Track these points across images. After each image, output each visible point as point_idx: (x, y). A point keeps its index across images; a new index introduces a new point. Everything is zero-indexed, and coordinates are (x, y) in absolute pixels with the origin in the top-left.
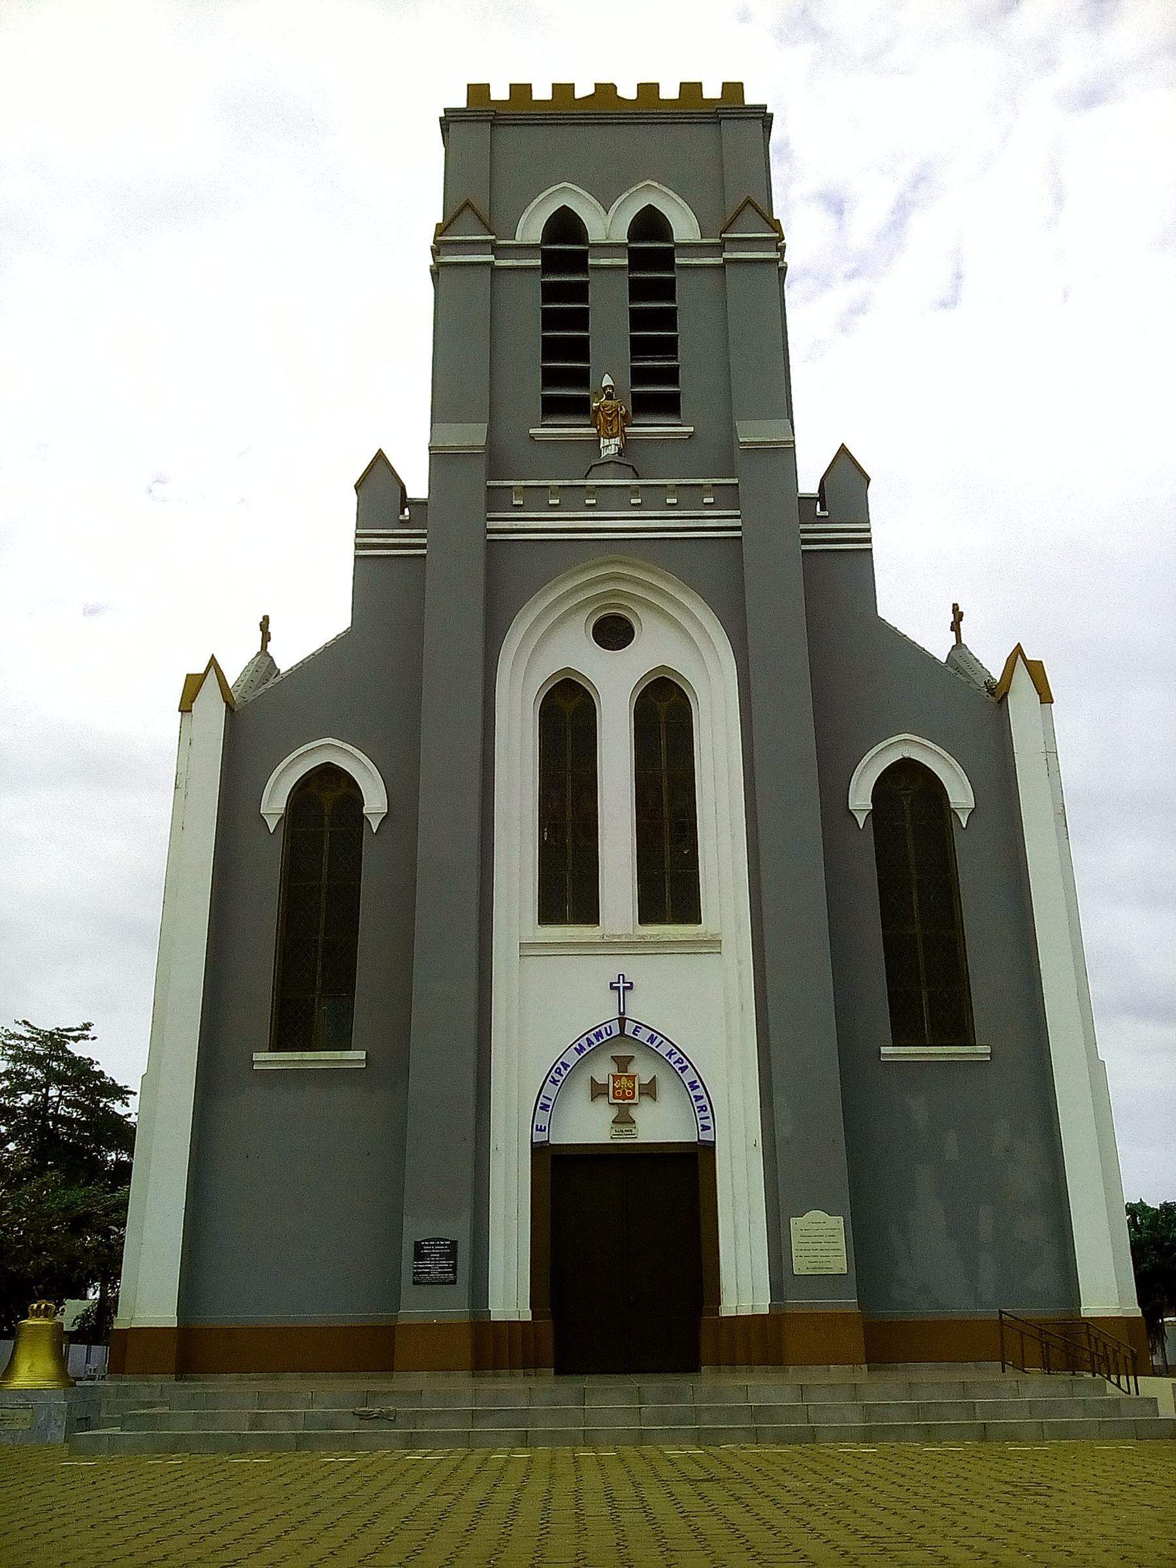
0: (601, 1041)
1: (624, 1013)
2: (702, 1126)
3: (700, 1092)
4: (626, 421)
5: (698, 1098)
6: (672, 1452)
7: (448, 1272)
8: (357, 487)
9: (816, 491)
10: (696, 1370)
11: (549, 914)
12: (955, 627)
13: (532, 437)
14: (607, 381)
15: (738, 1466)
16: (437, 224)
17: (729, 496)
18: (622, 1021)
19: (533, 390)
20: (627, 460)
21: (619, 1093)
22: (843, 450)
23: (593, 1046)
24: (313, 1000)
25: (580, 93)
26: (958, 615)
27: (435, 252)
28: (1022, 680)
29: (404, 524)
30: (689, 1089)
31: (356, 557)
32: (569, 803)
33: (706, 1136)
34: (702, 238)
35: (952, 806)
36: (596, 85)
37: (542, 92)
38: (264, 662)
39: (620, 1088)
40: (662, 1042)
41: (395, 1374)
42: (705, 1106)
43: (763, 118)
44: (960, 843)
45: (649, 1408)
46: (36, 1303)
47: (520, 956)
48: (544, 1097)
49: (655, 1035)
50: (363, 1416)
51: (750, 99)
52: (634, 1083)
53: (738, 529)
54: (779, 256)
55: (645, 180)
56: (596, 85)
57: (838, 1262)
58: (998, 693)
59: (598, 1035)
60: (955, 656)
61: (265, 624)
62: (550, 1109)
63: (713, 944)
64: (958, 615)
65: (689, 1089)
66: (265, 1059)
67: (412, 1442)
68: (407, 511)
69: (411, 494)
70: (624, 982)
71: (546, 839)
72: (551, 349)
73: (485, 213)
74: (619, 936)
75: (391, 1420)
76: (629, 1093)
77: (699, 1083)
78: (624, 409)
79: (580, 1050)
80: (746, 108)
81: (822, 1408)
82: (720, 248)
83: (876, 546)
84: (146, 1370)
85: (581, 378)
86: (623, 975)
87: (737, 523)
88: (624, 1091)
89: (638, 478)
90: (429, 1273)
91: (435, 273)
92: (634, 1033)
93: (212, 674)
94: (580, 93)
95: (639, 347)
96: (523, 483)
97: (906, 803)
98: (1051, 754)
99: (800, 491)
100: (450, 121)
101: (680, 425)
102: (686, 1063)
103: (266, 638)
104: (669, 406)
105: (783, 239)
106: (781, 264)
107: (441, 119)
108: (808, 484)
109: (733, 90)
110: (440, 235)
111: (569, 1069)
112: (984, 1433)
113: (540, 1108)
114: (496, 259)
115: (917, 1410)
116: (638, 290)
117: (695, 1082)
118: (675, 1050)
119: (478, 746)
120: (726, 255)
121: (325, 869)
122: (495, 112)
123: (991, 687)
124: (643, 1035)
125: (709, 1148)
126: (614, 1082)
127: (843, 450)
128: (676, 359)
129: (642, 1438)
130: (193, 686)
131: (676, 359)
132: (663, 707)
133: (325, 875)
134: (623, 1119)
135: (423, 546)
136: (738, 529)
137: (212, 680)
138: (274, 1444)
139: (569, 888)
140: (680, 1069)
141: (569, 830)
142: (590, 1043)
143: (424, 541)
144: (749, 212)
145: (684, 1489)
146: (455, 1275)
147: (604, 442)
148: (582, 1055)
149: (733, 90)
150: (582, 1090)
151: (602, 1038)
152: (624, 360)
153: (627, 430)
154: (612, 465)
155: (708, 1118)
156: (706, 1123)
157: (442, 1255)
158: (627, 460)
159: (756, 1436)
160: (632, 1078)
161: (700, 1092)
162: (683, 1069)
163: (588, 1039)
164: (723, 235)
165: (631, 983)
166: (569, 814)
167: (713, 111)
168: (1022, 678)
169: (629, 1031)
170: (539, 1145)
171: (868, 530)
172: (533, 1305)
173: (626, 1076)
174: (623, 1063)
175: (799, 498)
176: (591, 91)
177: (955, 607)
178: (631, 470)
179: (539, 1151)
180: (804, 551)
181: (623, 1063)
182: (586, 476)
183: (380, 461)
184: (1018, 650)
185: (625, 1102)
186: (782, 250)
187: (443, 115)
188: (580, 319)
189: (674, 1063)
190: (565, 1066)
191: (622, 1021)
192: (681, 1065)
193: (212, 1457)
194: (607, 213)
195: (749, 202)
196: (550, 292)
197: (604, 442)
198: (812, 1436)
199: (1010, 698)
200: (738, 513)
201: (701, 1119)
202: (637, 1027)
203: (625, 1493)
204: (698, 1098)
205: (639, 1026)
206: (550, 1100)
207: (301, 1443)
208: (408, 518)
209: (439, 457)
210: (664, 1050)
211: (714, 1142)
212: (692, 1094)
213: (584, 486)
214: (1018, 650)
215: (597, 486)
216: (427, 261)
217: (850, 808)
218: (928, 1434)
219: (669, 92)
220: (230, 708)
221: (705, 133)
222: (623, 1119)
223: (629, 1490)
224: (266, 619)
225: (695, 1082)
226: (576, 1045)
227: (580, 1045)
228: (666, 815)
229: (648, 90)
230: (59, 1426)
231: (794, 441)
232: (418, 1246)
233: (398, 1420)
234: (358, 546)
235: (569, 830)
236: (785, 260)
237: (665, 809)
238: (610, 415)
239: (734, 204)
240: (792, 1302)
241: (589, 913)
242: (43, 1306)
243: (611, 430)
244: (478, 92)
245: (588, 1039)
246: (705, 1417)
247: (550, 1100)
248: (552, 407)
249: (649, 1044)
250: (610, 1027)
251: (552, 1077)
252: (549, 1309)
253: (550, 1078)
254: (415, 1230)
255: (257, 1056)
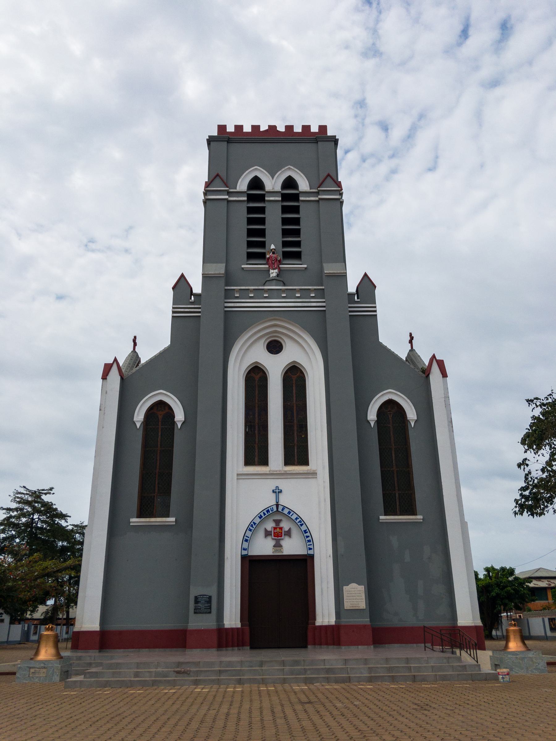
0: (269, 513)
1: (278, 502)
2: (309, 548)
3: (308, 534)
4: (280, 262)
5: (307, 537)
6: (296, 688)
7: (208, 609)
8: (173, 288)
9: (355, 291)
10: (305, 647)
11: (248, 462)
12: (411, 342)
13: (243, 268)
14: (273, 247)
15: (320, 695)
16: (206, 182)
17: (321, 294)
18: (277, 505)
19: (243, 249)
20: (279, 279)
21: (276, 535)
22: (366, 275)
23: (266, 516)
24: (154, 496)
25: (262, 129)
26: (412, 338)
27: (205, 194)
28: (435, 369)
29: (192, 303)
30: (304, 533)
31: (173, 317)
32: (256, 416)
33: (311, 552)
34: (310, 189)
35: (408, 419)
36: (269, 126)
37: (247, 129)
38: (134, 357)
39: (276, 532)
40: (293, 514)
41: (187, 650)
42: (310, 540)
43: (335, 141)
44: (412, 434)
45: (287, 668)
46: (47, 625)
47: (237, 479)
48: (246, 536)
49: (291, 511)
50: (178, 672)
51: (330, 133)
52: (282, 530)
53: (324, 307)
54: (340, 197)
55: (288, 165)
56: (269, 126)
57: (362, 604)
58: (426, 372)
59: (268, 511)
60: (411, 354)
61: (134, 341)
62: (248, 541)
63: (313, 474)
64: (412, 338)
65: (304, 533)
66: (135, 521)
67: (196, 683)
68: (193, 298)
69: (194, 291)
70: (278, 490)
71: (247, 431)
72: (250, 233)
73: (225, 178)
74: (276, 471)
75: (188, 674)
76: (280, 535)
77: (308, 531)
78: (279, 258)
79: (260, 517)
80: (328, 137)
81: (353, 668)
82: (318, 193)
83: (378, 313)
84: (87, 648)
85: (262, 245)
86: (278, 487)
87: (324, 304)
88: (278, 534)
89: (284, 285)
90: (200, 609)
91: (205, 202)
92: (282, 510)
93: (115, 365)
94: (262, 129)
95: (285, 233)
96: (239, 288)
97: (390, 417)
98: (447, 398)
99: (349, 291)
100: (211, 140)
101: (301, 264)
102: (303, 522)
103: (135, 344)
104: (297, 256)
105: (342, 190)
106: (341, 200)
107: (207, 140)
108: (352, 288)
109: (323, 129)
110: (207, 187)
111: (256, 525)
112: (414, 679)
113: (245, 541)
114: (229, 197)
115: (390, 669)
116: (285, 209)
117: (306, 530)
118: (298, 517)
119: (221, 394)
120: (320, 197)
121: (159, 444)
122: (229, 137)
123: (423, 371)
124: (286, 511)
125: (312, 557)
126: (274, 530)
127: (366, 275)
128: (299, 237)
129: (284, 681)
130: (107, 368)
131: (299, 237)
132: (294, 377)
133: (159, 446)
134: (278, 545)
135: (199, 312)
136: (324, 307)
137: (115, 367)
138: (143, 684)
139: (257, 451)
140: (300, 525)
141: (257, 427)
142: (264, 514)
143: (200, 310)
144: (329, 179)
145: (299, 707)
146: (211, 610)
147: (271, 271)
148: (261, 519)
149: (323, 129)
150: (261, 534)
151: (269, 512)
152: (279, 239)
153: (281, 266)
154: (274, 281)
155: (311, 545)
156: (310, 547)
157: (205, 601)
158: (279, 279)
159: (328, 680)
160: (281, 528)
161: (308, 534)
162: (302, 525)
163: (264, 513)
164: (318, 189)
165: (281, 490)
166: (257, 421)
167: (315, 138)
168: (435, 369)
169: (280, 509)
170: (244, 556)
171: (375, 307)
172: (241, 621)
173: (279, 528)
174: (278, 522)
175: (348, 294)
176: (267, 128)
177: (411, 334)
178: (282, 282)
179: (244, 558)
180: (350, 315)
181: (278, 522)
182: (264, 284)
183: (183, 278)
184: (434, 356)
185: (279, 538)
186: (341, 194)
187: (208, 138)
188: (262, 221)
189: (298, 522)
190: (255, 524)
191: (277, 505)
192: (301, 523)
193: (120, 690)
194: (273, 179)
195: (329, 175)
196: (250, 210)
197: (271, 271)
198: (349, 680)
199: (430, 375)
200: (324, 300)
201: (308, 545)
202: (283, 508)
203: (278, 709)
204: (307, 537)
205: (284, 507)
206: (249, 537)
207: (154, 683)
208: (193, 301)
209: (206, 277)
210: (294, 517)
211: (314, 555)
212: (305, 535)
213: (263, 289)
214: (434, 356)
215: (269, 289)
216: (202, 197)
217: (369, 419)
218: (393, 679)
219: (298, 129)
220: (122, 378)
221: (312, 146)
222: (278, 545)
223: (279, 708)
224: (135, 337)
225: (306, 530)
226: (259, 515)
227: (260, 515)
228: (295, 422)
229: (289, 128)
230: (57, 675)
231: (346, 273)
232: (196, 598)
233: (191, 674)
234: (173, 312)
235: (257, 427)
236: (343, 198)
237: (295, 418)
238: (274, 260)
239: (323, 176)
240: (345, 621)
241: (264, 462)
242: (50, 627)
243: (274, 266)
244: (222, 128)
245: (264, 513)
246: (309, 672)
247: (249, 537)
248: (250, 256)
249: (288, 515)
250: (273, 508)
251: (249, 528)
252: (248, 623)
253: (248, 529)
254: (195, 591)
255: (133, 520)
